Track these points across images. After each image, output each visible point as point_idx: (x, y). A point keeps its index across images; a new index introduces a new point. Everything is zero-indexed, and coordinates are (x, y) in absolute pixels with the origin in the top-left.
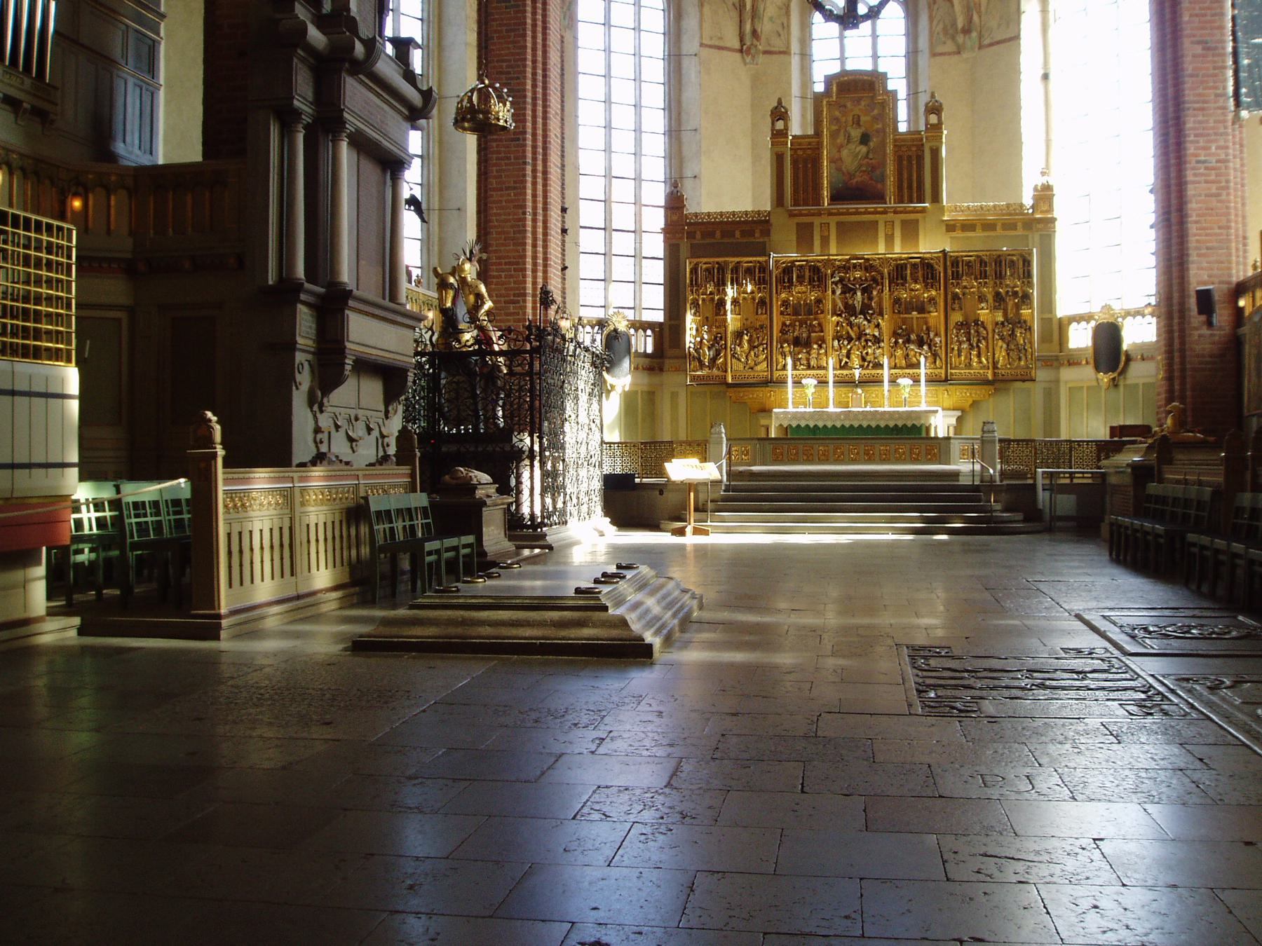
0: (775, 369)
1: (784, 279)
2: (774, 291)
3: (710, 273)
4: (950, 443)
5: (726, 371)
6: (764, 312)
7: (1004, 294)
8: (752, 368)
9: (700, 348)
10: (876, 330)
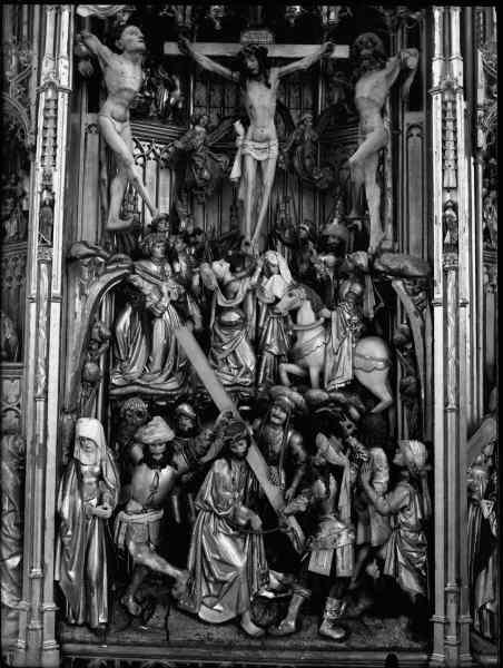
10: (375, 349)
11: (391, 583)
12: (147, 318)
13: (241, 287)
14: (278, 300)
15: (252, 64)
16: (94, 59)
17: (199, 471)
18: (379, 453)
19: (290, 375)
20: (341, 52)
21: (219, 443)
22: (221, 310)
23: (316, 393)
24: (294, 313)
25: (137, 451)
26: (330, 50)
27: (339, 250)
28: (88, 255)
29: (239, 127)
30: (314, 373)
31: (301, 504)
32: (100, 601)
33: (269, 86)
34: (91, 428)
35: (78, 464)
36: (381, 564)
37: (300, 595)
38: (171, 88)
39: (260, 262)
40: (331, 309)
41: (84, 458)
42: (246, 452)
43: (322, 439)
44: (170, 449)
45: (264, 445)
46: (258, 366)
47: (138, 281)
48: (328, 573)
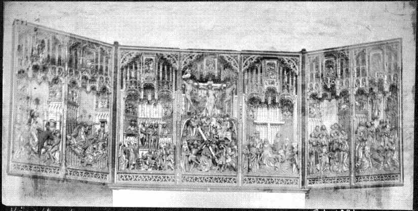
13: (208, 123)
17: (202, 150)
18: (230, 149)
19: (216, 138)
21: (205, 145)
23: (220, 139)
24: (216, 127)
25: (192, 147)
45: (212, 147)
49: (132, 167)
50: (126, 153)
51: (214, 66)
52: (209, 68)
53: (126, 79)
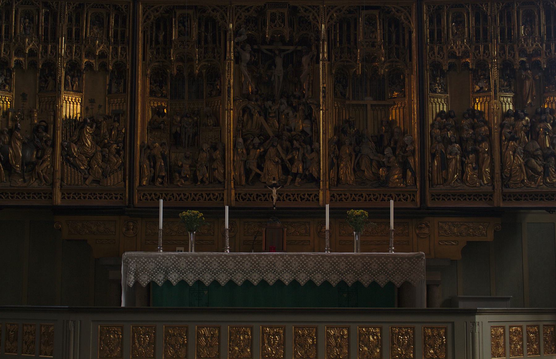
0: (137, 184)
1: (157, 37)
2: (140, 56)
3: (32, 20)
4: (474, 323)
5: (53, 184)
6: (121, 88)
7: (517, 67)
8: (98, 182)
9: (10, 143)
10: (307, 123)
11: (311, 175)
12: (251, 116)
14: (284, 111)
15: (277, 52)
16: (238, 52)
17: (265, 152)
18: (309, 148)
19: (287, 129)
20: (299, 48)
22: (269, 113)
23: (293, 133)
24: (288, 114)
25: (251, 147)
26: (296, 48)
27: (299, 98)
28: (238, 99)
29: (273, 67)
30: (293, 128)
31: (290, 156)
32: (243, 178)
33: (281, 58)
34: (241, 140)
35: (237, 149)
36: (309, 171)
37: (290, 177)
38: (255, 57)
39: (279, 101)
40: (297, 112)
41: (238, 147)
42: (277, 145)
43: (295, 142)
44: (261, 144)
45: (281, 146)
46: (279, 127)
47: (250, 106)
48: (296, 172)
49: (160, 180)
50: (153, 159)
51: (283, 22)
52: (275, 26)
53: (151, 44)
